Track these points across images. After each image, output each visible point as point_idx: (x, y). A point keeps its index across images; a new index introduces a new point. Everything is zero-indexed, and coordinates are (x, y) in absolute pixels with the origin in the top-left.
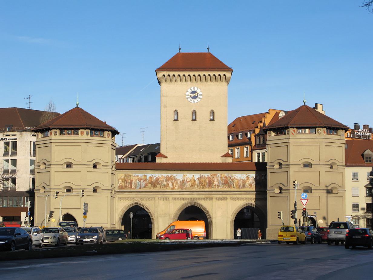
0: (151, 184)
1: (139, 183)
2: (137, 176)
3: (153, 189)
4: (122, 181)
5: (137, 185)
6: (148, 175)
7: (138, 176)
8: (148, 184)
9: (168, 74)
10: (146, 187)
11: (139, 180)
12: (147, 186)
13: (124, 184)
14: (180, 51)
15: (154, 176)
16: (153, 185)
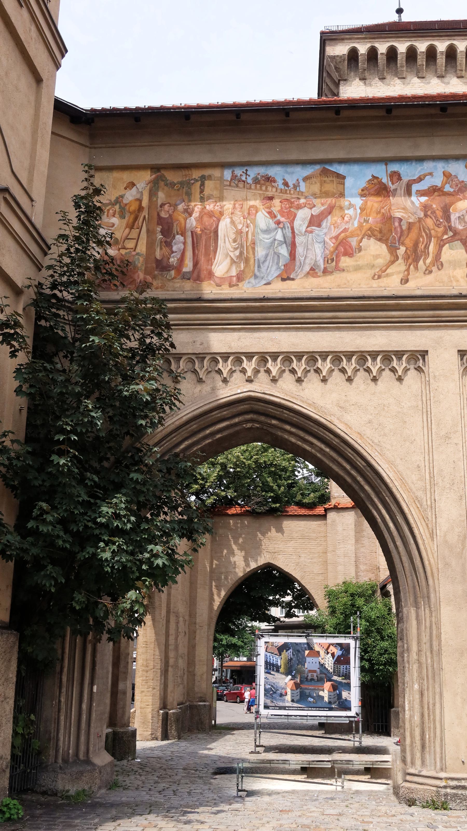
0: (380, 240)
1: (279, 236)
2: (256, 181)
3: (405, 281)
4: (131, 227)
5: (260, 252)
6: (355, 168)
7: (269, 179)
8: (354, 242)
9: (369, 45)
10: (338, 269)
11: (272, 215)
12: (349, 253)
13: (142, 248)
14: (400, 17)
15: (405, 179)
16: (402, 250)
